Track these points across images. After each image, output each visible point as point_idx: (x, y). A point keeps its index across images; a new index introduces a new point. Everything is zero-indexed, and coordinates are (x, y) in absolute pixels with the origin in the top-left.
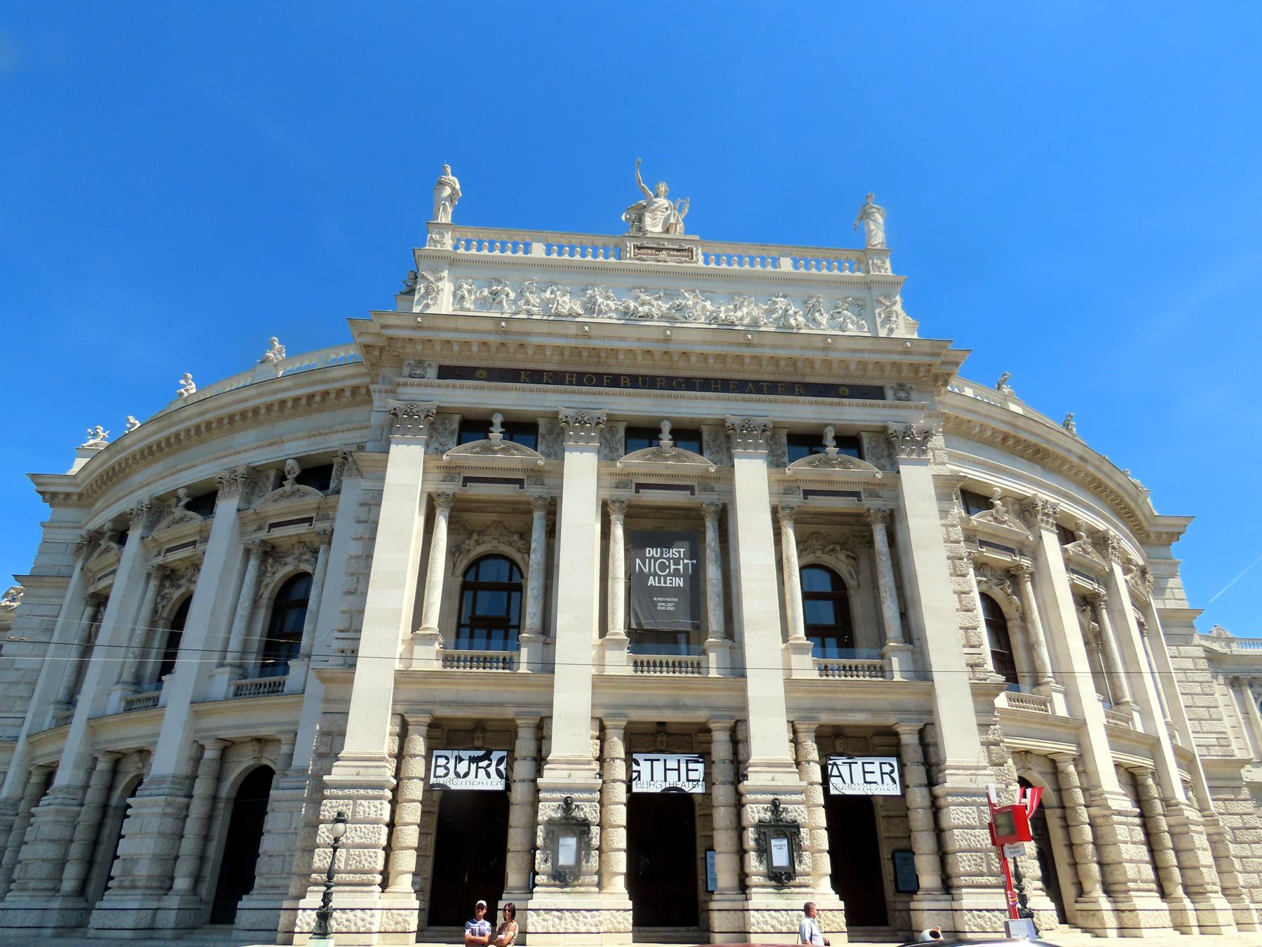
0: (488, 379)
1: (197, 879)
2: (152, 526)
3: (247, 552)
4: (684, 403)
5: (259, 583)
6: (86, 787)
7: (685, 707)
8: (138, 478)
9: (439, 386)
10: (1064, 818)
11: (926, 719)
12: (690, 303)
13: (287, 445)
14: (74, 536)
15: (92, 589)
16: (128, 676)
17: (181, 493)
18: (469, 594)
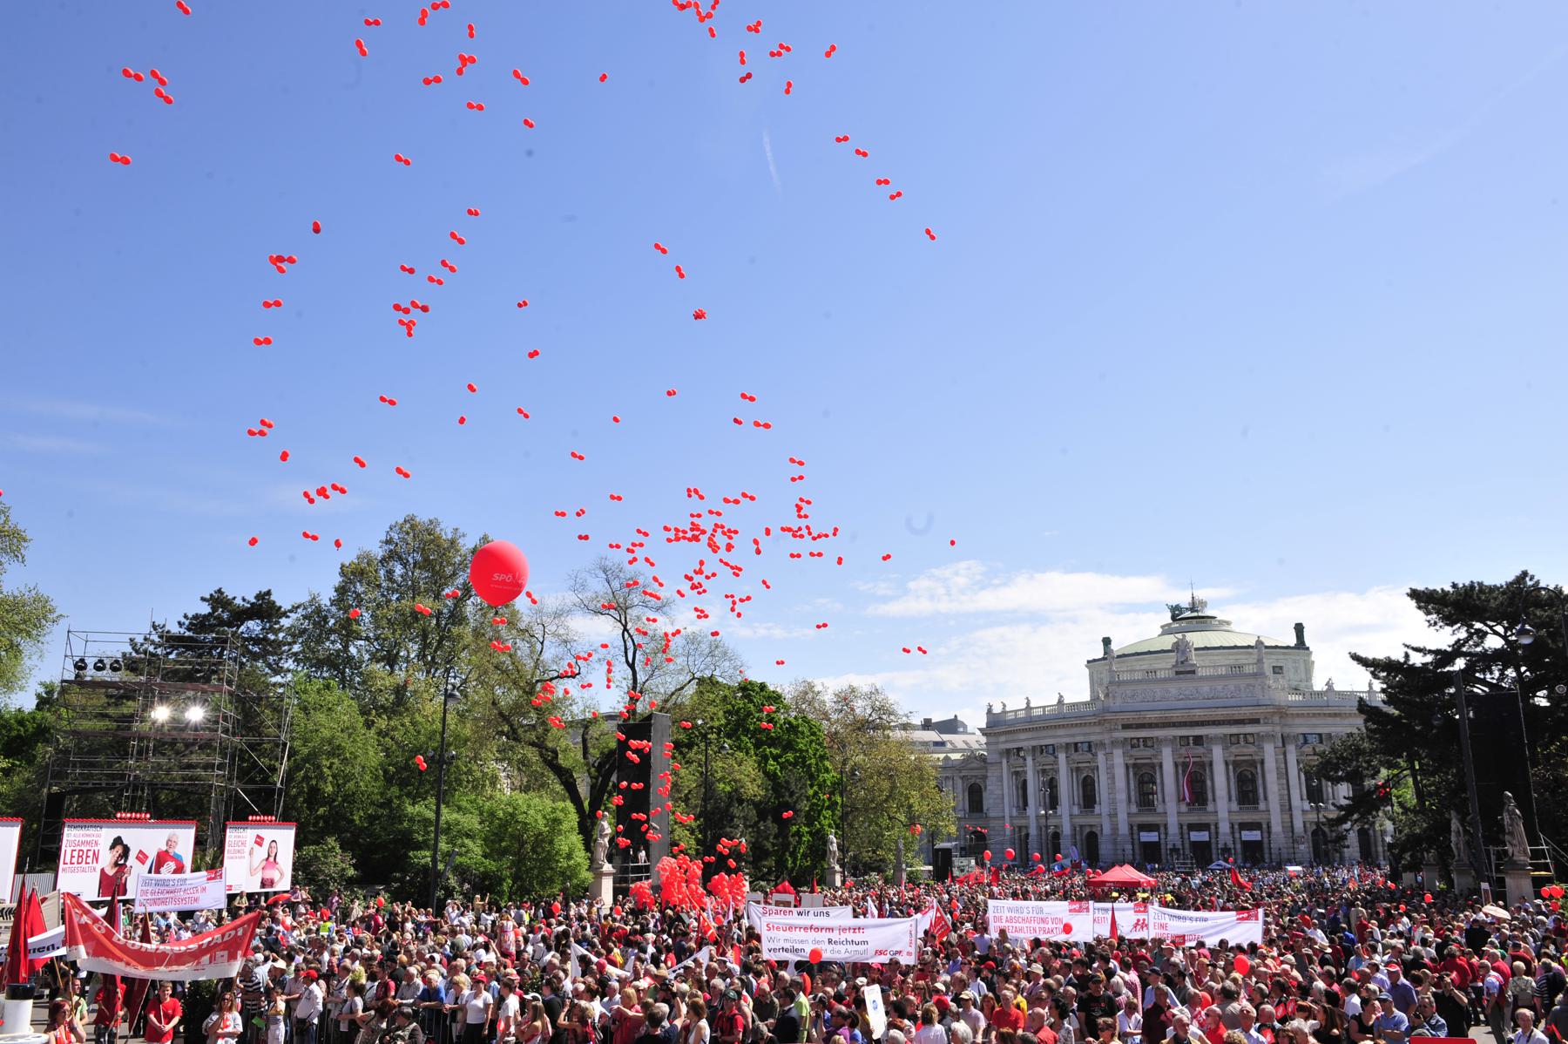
8: (1023, 736)
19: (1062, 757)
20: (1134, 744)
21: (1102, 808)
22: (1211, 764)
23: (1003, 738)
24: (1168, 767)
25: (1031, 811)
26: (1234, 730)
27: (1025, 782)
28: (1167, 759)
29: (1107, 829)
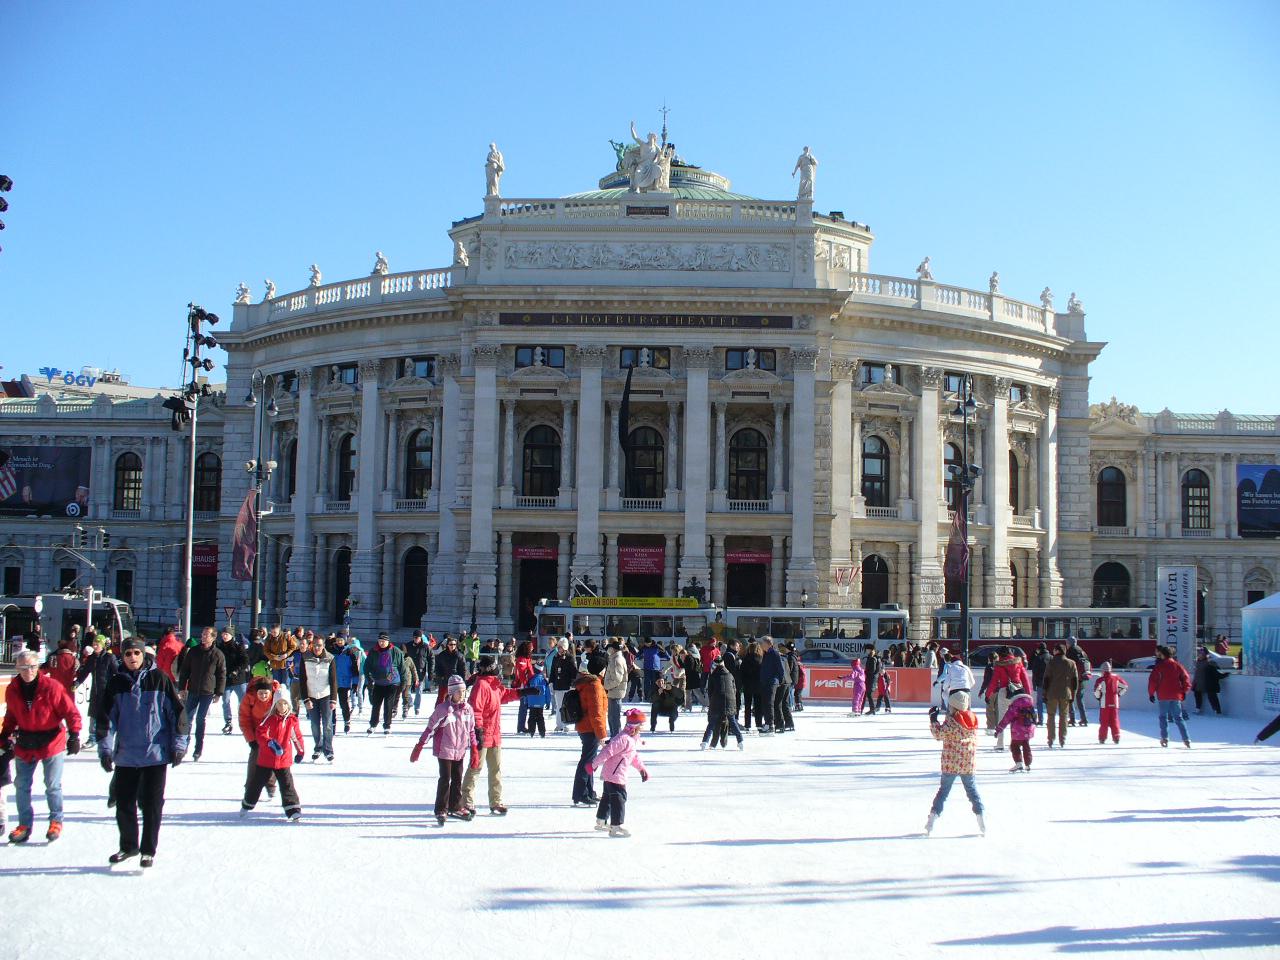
1: (394, 606)
2: (315, 388)
3: (387, 416)
4: (657, 335)
5: (398, 437)
6: (314, 553)
7: (650, 528)
8: (298, 347)
9: (501, 330)
10: (896, 579)
11: (787, 533)
12: (665, 254)
13: (404, 347)
16: (322, 489)
17: (335, 368)
19: (370, 387)
20: (522, 355)
21: (440, 498)
22: (681, 410)
23: (260, 355)
24: (591, 412)
25: (299, 504)
26: (736, 338)
27: (295, 443)
28: (591, 392)
29: (448, 541)
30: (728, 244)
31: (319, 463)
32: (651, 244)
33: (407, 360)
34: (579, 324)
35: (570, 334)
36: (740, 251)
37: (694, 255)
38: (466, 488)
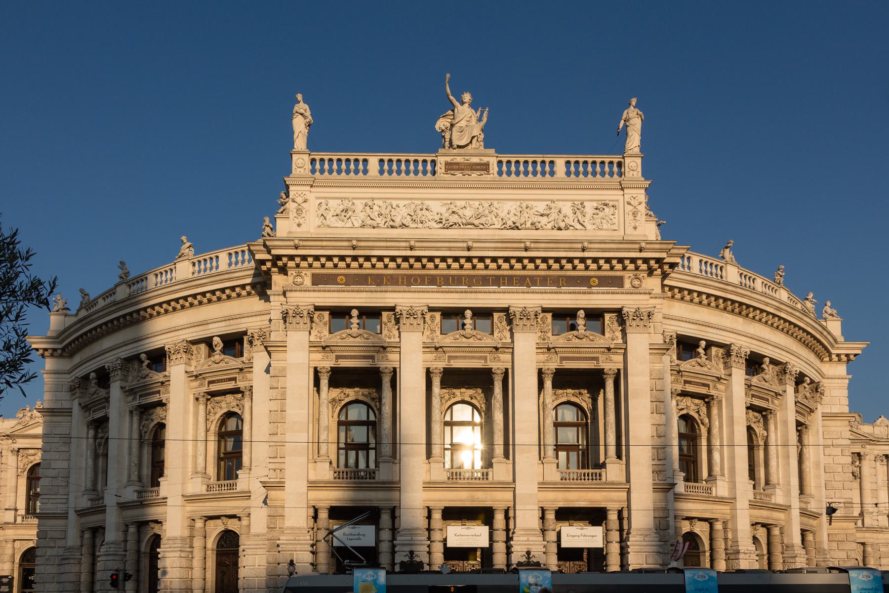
0: (346, 284)
2: (124, 379)
5: (207, 420)
6: (126, 541)
8: (107, 343)
12: (487, 212)
13: (211, 326)
14: (68, 379)
15: (90, 418)
17: (143, 356)
18: (343, 428)
23: (77, 359)
30: (553, 201)
31: (130, 454)
32: (471, 203)
33: (215, 338)
34: (397, 284)
35: (388, 295)
36: (567, 209)
37: (519, 214)
38: (278, 460)
